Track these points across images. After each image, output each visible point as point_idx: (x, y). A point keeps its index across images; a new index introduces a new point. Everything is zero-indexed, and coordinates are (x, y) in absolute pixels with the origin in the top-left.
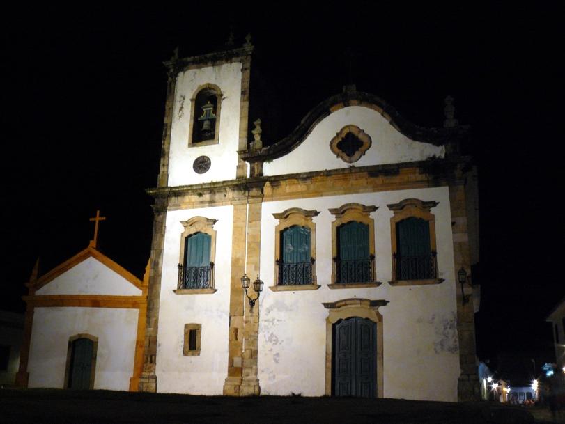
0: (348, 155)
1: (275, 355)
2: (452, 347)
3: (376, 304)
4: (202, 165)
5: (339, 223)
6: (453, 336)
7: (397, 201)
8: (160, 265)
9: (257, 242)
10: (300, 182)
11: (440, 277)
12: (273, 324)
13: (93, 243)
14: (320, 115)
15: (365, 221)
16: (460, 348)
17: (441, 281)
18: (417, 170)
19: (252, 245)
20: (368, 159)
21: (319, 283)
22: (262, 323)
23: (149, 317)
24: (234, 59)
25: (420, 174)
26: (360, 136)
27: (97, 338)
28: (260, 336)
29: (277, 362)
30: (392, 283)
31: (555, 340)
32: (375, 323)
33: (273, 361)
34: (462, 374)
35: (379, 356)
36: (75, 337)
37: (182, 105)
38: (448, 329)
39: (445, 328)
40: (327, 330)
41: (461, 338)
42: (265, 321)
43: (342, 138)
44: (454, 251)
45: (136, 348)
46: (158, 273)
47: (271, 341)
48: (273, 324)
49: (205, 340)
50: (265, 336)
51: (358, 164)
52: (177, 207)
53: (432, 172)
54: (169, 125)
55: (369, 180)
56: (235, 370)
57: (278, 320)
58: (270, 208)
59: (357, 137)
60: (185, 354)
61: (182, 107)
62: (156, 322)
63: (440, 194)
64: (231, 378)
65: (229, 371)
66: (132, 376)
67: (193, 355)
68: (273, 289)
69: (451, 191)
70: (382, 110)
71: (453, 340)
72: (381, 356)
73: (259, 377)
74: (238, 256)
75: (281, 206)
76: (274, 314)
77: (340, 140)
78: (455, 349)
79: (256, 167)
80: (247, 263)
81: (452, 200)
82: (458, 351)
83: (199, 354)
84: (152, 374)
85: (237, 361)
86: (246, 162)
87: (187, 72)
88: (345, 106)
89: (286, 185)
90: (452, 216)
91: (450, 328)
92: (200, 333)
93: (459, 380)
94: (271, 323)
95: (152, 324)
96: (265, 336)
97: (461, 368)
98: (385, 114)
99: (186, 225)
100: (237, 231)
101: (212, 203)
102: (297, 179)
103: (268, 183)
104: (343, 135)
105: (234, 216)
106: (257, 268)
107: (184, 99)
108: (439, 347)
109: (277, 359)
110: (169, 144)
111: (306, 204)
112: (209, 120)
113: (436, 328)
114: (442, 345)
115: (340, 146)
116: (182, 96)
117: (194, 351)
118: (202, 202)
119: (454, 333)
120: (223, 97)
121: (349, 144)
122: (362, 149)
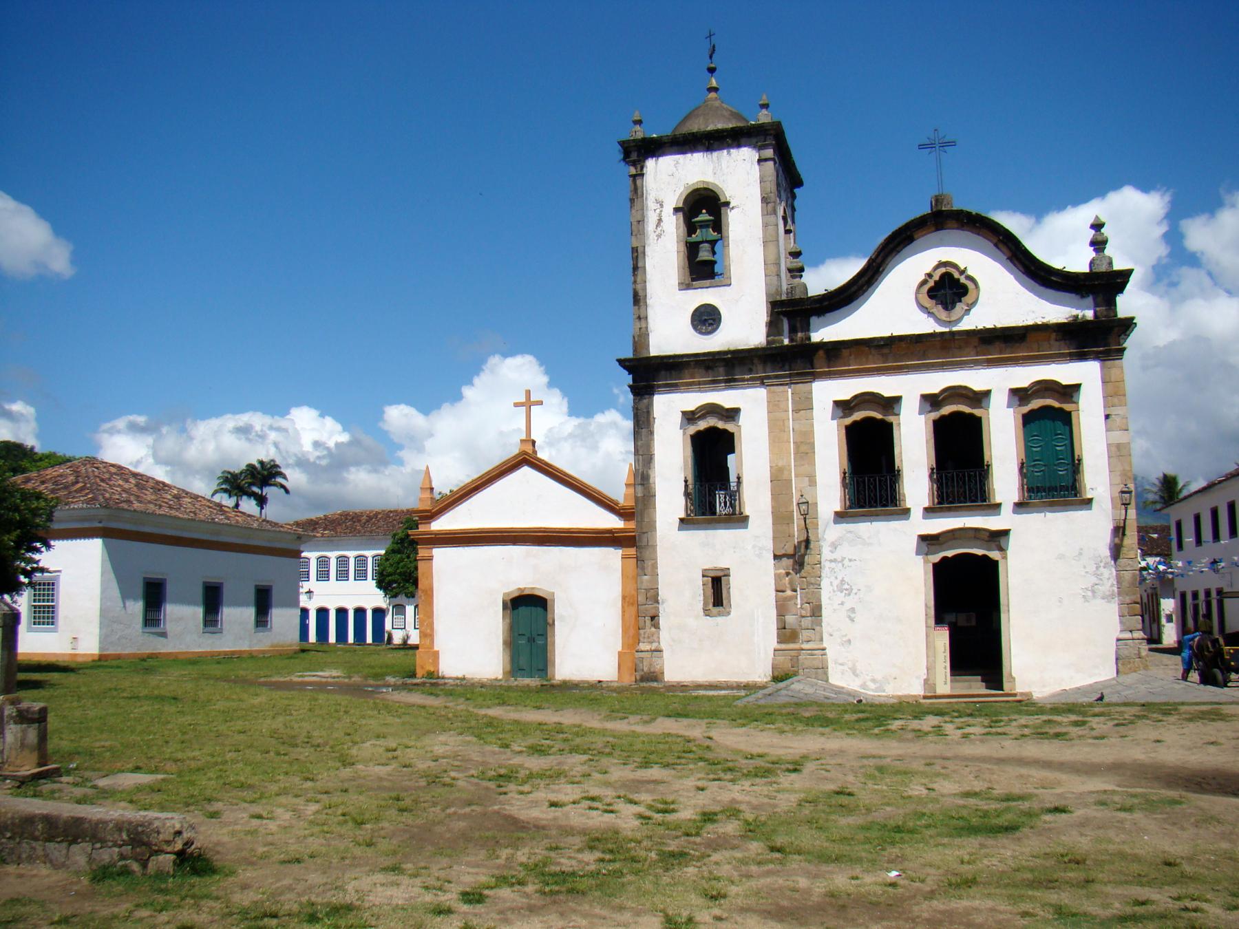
0: (946, 308)
1: (848, 610)
2: (1108, 593)
3: (999, 538)
4: (706, 319)
5: (935, 415)
6: (1109, 579)
7: (1025, 384)
8: (651, 481)
9: (809, 443)
10: (873, 351)
11: (1089, 496)
12: (843, 565)
14: (899, 244)
15: (977, 412)
16: (1119, 594)
17: (1089, 502)
18: (1054, 336)
19: (804, 448)
20: (977, 318)
22: (826, 565)
23: (639, 560)
24: (743, 141)
25: (1056, 340)
26: (963, 280)
27: (553, 593)
28: (825, 583)
29: (852, 620)
30: (1020, 506)
31: (1174, 544)
32: (997, 561)
33: (847, 619)
34: (1121, 631)
35: (1003, 608)
36: (512, 592)
37: (660, 215)
38: (1102, 569)
39: (1097, 568)
40: (926, 573)
41: (1119, 580)
42: (831, 561)
43: (936, 282)
44: (1109, 457)
45: (623, 607)
46: (649, 492)
47: (842, 592)
48: (843, 565)
49: (736, 589)
50: (831, 583)
52: (673, 388)
54: (640, 250)
55: (979, 349)
56: (786, 634)
57: (850, 560)
59: (958, 280)
60: (707, 612)
61: (660, 220)
62: (655, 566)
64: (783, 646)
65: (779, 636)
66: (620, 649)
67: (719, 614)
68: (840, 517)
69: (1102, 368)
70: (995, 241)
71: (1109, 584)
72: (1007, 609)
73: (825, 645)
74: (780, 465)
75: (848, 388)
76: (844, 551)
77: (931, 283)
78: (1112, 596)
79: (798, 325)
80: (796, 476)
81: (1104, 382)
82: (1116, 599)
83: (729, 613)
84: (654, 646)
85: (790, 619)
86: (781, 317)
87: (661, 159)
88: (937, 229)
89: (850, 355)
90: (1104, 407)
91: (1104, 567)
92: (729, 583)
93: (1118, 640)
94: (840, 564)
95: (648, 571)
96: (831, 583)
97: (1121, 622)
98: (1001, 245)
99: (690, 416)
100: (776, 427)
102: (868, 347)
103: (821, 353)
104: (936, 277)
105: (768, 402)
106: (813, 482)
107: (662, 206)
108: (1089, 593)
109: (853, 615)
110: (645, 282)
111: (884, 385)
112: (707, 242)
113: (1085, 567)
114: (1093, 592)
115: (932, 293)
116: (657, 201)
117: (720, 609)
118: (714, 382)
119: (1111, 574)
120: (731, 206)
122: (965, 299)
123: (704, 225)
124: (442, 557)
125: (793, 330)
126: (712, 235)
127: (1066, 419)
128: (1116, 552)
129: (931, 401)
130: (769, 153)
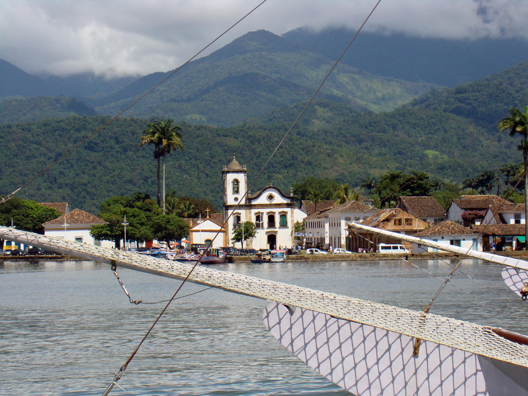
3: (276, 232)
4: (236, 199)
7: (280, 211)
13: (208, 217)
20: (274, 202)
21: (264, 227)
30: (279, 228)
51: (273, 203)
53: (288, 205)
58: (254, 211)
63: (288, 210)
85: (248, 243)
100: (246, 216)
101: (240, 209)
111: (261, 210)
115: (268, 198)
121: (271, 197)
123: (235, 184)
124: (194, 234)
125: (249, 202)
126: (237, 186)
127: (285, 216)
128: (291, 235)
129: (268, 213)
130: (246, 174)
